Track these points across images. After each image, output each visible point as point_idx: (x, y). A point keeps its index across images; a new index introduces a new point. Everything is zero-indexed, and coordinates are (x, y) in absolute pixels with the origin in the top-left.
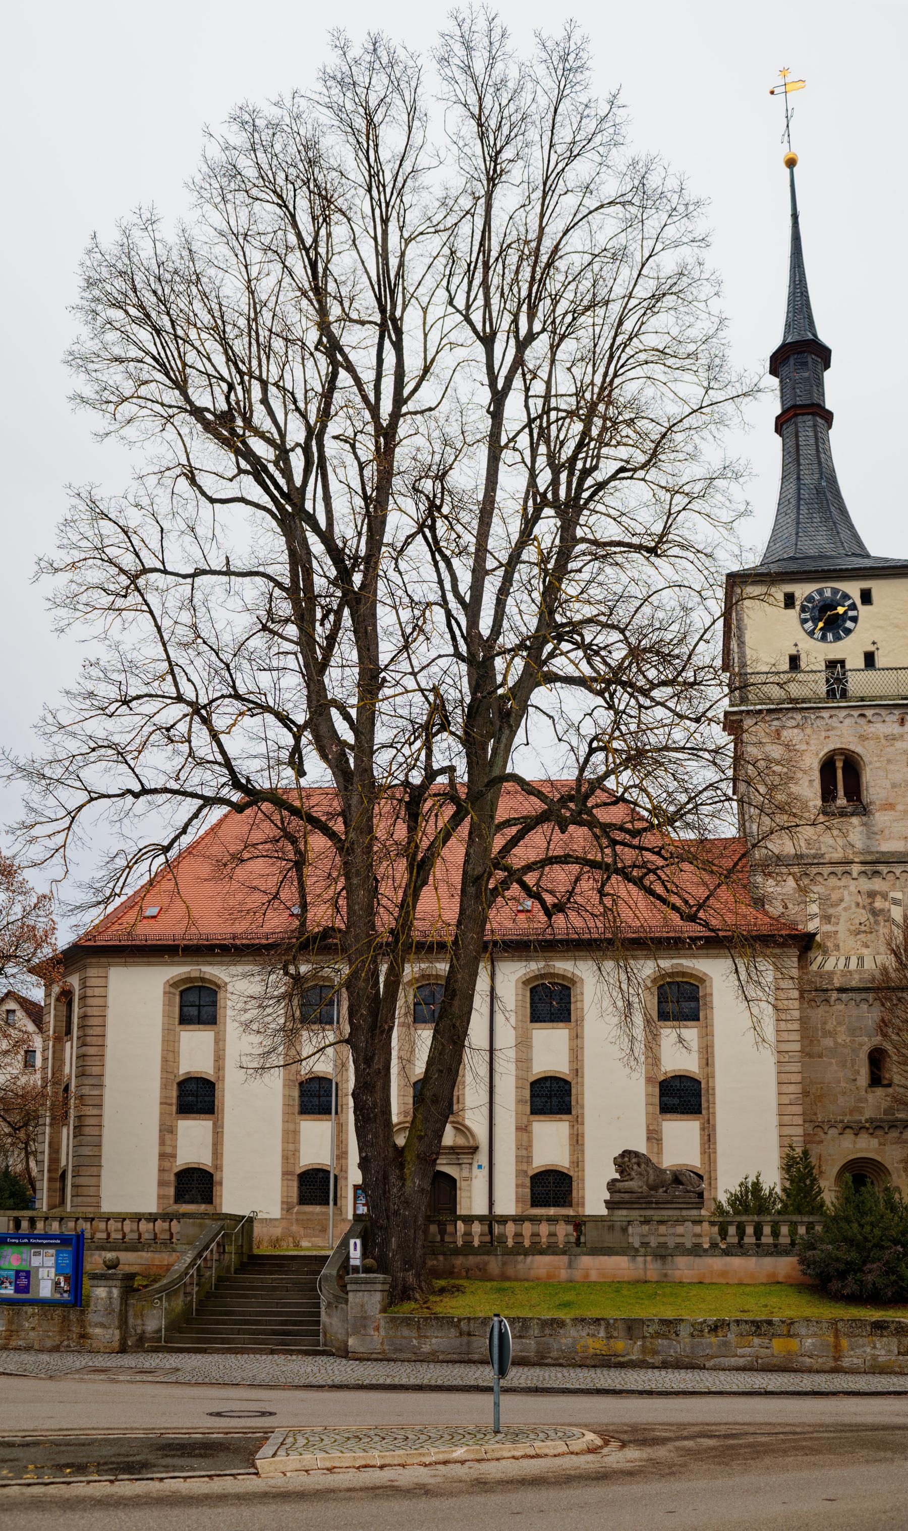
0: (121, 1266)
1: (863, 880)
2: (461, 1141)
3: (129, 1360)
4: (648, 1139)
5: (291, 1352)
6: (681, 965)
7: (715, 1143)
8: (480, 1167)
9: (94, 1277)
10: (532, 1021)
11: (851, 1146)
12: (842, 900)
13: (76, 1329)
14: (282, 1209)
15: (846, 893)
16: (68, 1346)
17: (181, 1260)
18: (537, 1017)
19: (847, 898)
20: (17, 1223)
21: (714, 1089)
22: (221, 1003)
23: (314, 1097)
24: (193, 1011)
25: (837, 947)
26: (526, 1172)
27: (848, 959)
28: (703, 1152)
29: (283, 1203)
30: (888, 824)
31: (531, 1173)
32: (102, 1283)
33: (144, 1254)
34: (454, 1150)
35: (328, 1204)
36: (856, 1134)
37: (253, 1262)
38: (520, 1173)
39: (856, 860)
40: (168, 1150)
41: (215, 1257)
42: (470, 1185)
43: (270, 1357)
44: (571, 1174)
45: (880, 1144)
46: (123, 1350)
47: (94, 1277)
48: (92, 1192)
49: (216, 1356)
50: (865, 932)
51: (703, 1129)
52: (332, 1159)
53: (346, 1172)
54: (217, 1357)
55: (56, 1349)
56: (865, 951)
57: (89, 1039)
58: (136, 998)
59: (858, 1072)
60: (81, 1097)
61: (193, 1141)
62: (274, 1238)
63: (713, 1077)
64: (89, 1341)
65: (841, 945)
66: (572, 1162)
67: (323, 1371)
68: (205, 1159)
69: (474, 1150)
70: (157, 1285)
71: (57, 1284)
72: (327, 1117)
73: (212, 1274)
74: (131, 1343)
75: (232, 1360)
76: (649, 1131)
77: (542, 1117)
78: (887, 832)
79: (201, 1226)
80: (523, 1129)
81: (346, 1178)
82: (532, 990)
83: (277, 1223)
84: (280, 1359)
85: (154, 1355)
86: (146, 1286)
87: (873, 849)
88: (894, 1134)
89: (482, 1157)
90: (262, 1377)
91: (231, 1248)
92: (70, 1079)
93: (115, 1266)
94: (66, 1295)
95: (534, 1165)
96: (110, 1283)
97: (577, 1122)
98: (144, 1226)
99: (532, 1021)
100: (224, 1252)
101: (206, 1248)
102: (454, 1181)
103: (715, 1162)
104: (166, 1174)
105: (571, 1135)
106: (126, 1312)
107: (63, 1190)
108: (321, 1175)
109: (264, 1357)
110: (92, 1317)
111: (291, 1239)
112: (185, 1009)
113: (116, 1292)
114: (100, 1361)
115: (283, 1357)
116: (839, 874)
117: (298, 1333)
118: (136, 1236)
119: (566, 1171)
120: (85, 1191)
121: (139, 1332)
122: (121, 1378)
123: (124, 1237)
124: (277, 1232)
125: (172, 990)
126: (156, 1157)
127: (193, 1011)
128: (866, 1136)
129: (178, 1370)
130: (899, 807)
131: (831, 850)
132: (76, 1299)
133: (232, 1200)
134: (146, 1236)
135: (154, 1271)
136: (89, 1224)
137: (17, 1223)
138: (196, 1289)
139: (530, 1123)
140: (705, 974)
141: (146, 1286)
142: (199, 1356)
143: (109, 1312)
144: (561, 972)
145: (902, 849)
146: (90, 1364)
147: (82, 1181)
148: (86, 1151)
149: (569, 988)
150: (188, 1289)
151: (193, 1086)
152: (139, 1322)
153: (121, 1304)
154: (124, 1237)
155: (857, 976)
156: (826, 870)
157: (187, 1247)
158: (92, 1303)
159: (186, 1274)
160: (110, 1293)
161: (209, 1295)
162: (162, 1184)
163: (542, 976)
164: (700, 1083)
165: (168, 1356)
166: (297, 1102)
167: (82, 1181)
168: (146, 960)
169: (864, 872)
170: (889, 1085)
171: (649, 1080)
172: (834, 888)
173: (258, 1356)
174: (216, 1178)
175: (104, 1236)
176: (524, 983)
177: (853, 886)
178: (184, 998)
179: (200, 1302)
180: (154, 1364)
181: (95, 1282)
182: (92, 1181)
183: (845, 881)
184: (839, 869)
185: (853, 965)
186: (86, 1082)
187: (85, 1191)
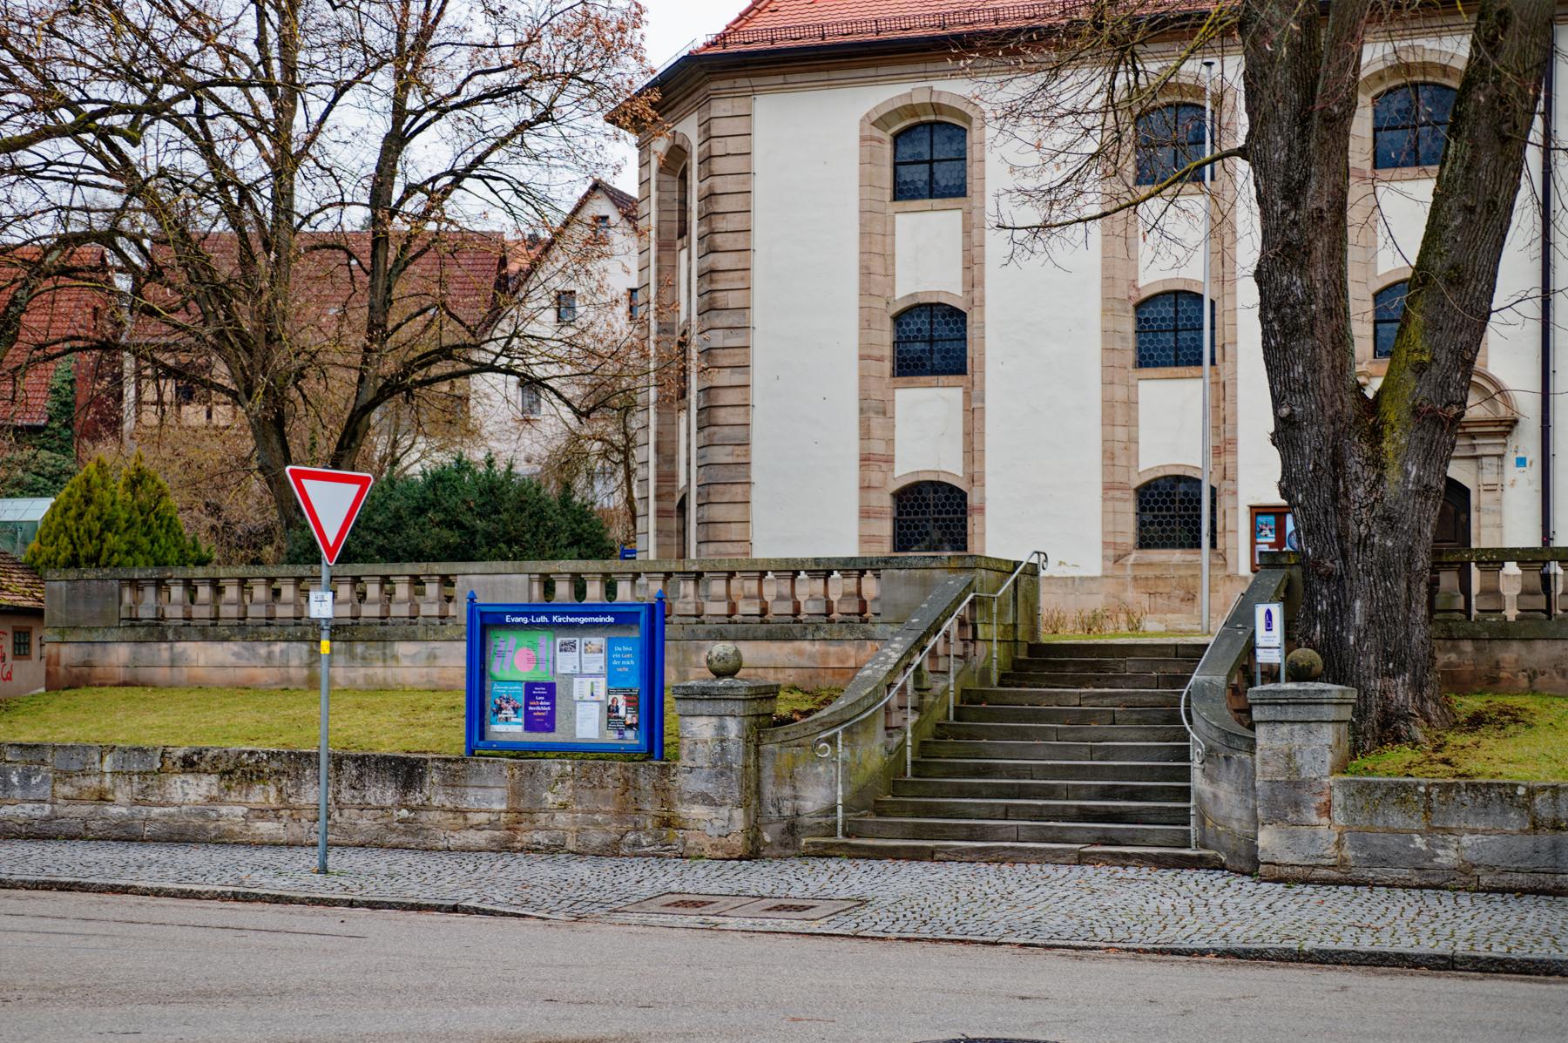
0: (741, 673)
3: (761, 878)
5: (1124, 860)
9: (687, 695)
13: (651, 807)
14: (1104, 557)
16: (637, 844)
17: (878, 658)
20: (548, 586)
22: (973, 153)
23: (1168, 331)
24: (919, 174)
29: (1105, 544)
32: (704, 707)
33: (806, 646)
35: (1199, 546)
37: (1039, 662)
40: (878, 447)
41: (956, 648)
43: (1077, 870)
46: (753, 853)
47: (687, 695)
48: (734, 532)
49: (954, 867)
54: (955, 872)
55: (611, 850)
57: (719, 239)
58: (808, 154)
60: (707, 353)
61: (927, 431)
62: (1088, 613)
64: (680, 833)
67: (1200, 910)
68: (947, 464)
70: (826, 711)
71: (612, 710)
72: (1193, 370)
73: (947, 688)
74: (772, 838)
75: (987, 878)
79: (926, 585)
83: (1094, 586)
84: (1097, 875)
85: (819, 864)
86: (808, 713)
90: (1055, 923)
91: (990, 631)
92: (689, 320)
93: (732, 673)
94: (630, 734)
96: (722, 707)
98: (807, 588)
100: (975, 638)
101: (934, 629)
104: (873, 495)
106: (759, 770)
107: (683, 532)
108: (1182, 487)
109: (1064, 870)
110: (691, 783)
111: (1123, 617)
112: (902, 169)
113: (733, 728)
114: (699, 879)
115: (1105, 871)
117: (1141, 816)
118: (787, 608)
120: (722, 532)
121: (787, 813)
122: (731, 923)
123: (764, 612)
124: (1095, 602)
126: (856, 462)
127: (919, 174)
129: (863, 903)
132: (654, 743)
133: (999, 535)
134: (808, 608)
135: (827, 681)
136: (691, 584)
137: (548, 586)
138: (912, 718)
141: (808, 713)
142: (917, 867)
143: (721, 769)
146: (675, 887)
147: (717, 512)
148: (720, 455)
150: (896, 720)
151: (921, 323)
152: (787, 791)
153: (747, 753)
154: (764, 612)
157: (896, 628)
158: (684, 752)
159: (890, 686)
160: (721, 728)
161: (942, 731)
162: (866, 514)
165: (847, 864)
166: (1131, 344)
167: (717, 512)
168: (824, 76)
173: (1049, 869)
174: (972, 500)
175: (723, 608)
178: (901, 149)
179: (922, 747)
180: (813, 888)
181: (690, 706)
182: (734, 513)
186: (717, 322)
187: (722, 532)
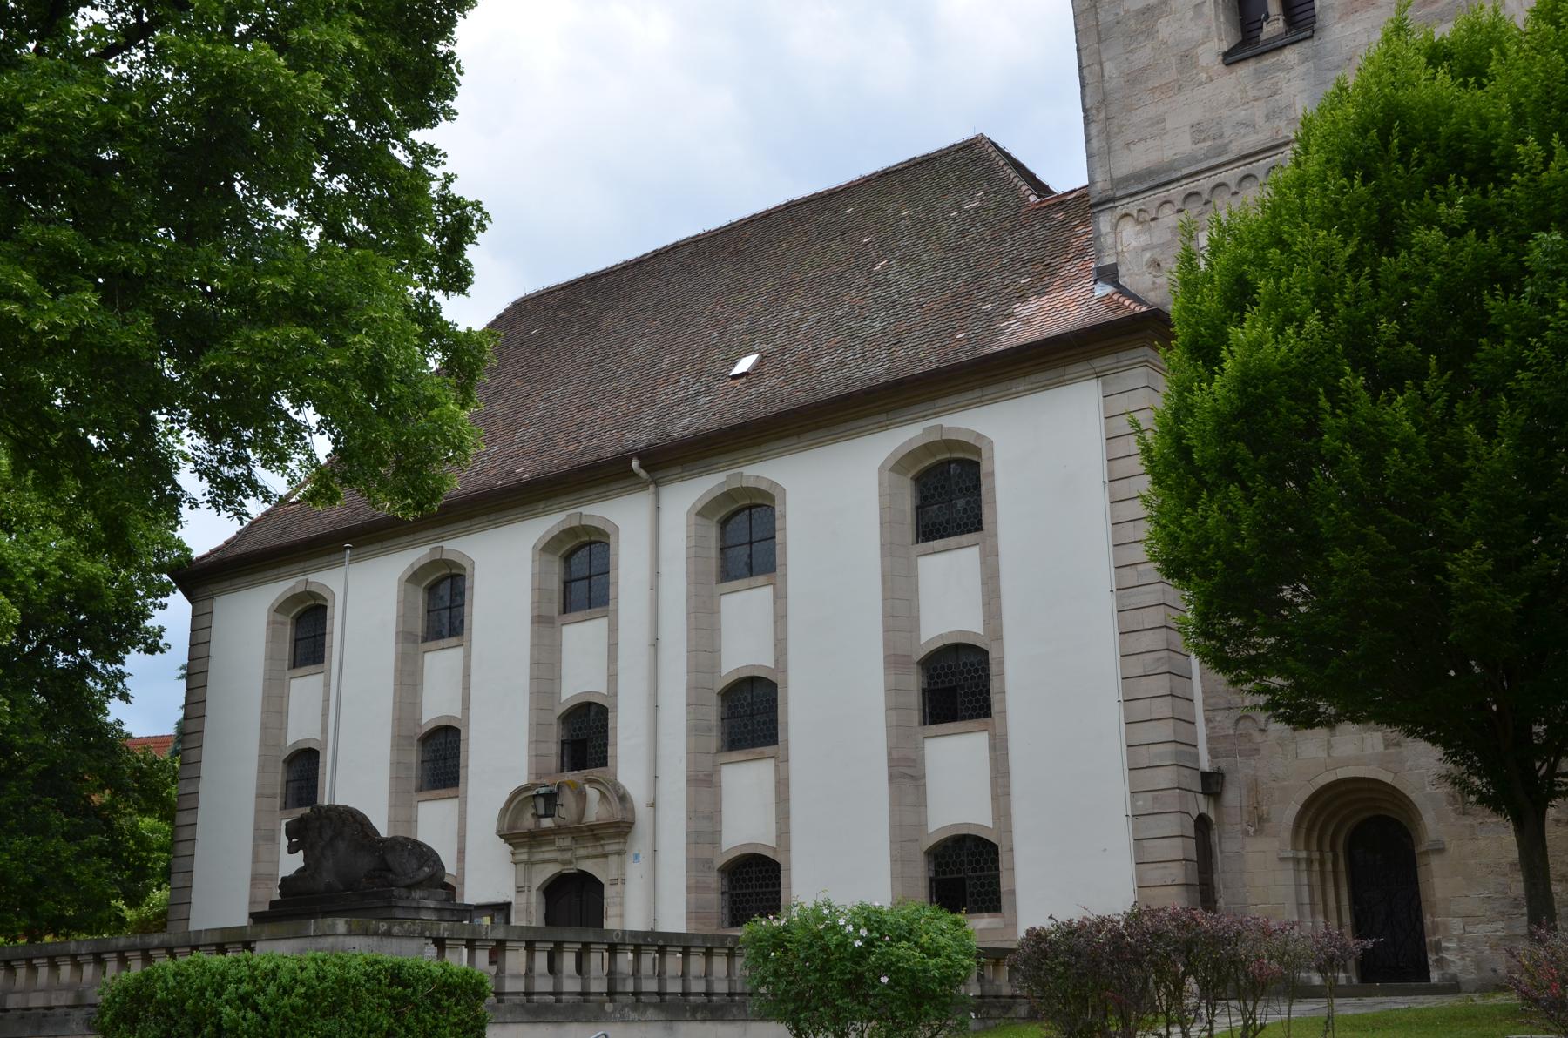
4: (891, 778)
11: (1322, 754)
26: (710, 861)
31: (720, 861)
76: (893, 762)
82: (724, 523)
95: (725, 848)
97: (782, 761)
119: (770, 854)
125: (280, 618)
131: (1243, 131)
144: (751, 484)
156: (1231, 175)
164: (984, 653)
171: (893, 661)
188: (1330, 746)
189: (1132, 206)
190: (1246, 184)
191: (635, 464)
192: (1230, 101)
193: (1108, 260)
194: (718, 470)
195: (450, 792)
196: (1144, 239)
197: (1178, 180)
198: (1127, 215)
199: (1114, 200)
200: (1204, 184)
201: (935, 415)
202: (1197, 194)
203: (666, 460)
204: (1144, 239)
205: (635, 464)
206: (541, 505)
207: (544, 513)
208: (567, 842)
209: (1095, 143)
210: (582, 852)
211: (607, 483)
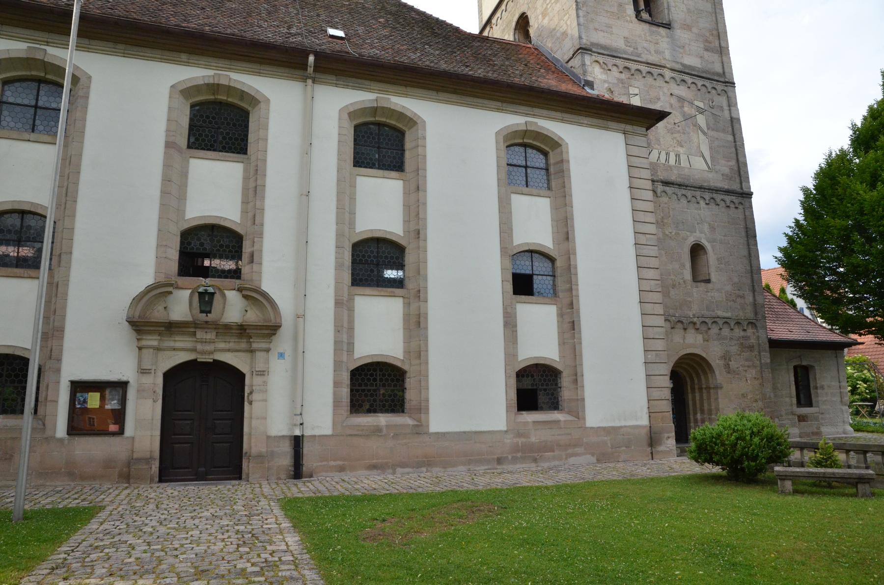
1: (673, 85)
2: (253, 316)
6: (536, 123)
7: (580, 332)
8: (281, 355)
10: (354, 166)
11: (682, 341)
12: (659, 99)
15: (661, 93)
18: (361, 161)
19: (662, 98)
21: (576, 268)
25: (658, 140)
27: (668, 154)
28: (562, 343)
30: (687, 41)
34: (242, 331)
36: (685, 329)
38: (338, 365)
39: (668, 66)
42: (265, 383)
44: (405, 367)
45: (705, 340)
50: (679, 132)
51: (561, 315)
52: (34, 343)
53: (59, 360)
56: (681, 150)
59: (683, 266)
63: (575, 254)
65: (661, 140)
66: (407, 352)
69: (271, 330)
77: (368, 290)
78: (687, 48)
80: (344, 307)
81: (58, 371)
82: (357, 128)
87: (678, 60)
88: (714, 330)
89: (283, 342)
99: (354, 166)
102: (243, 376)
103: (581, 355)
105: (407, 318)
116: (655, 75)
119: (399, 364)
128: (693, 331)
130: (694, 30)
139: (351, 299)
140: (560, 138)
145: (699, 66)
149: (402, 133)
155: (675, 172)
163: (375, 110)
169: (673, 78)
170: (708, 281)
172: (651, 86)
176: (350, 114)
177: (666, 89)
183: (660, 82)
184: (655, 71)
185: (672, 161)
188: (684, 338)
189: (601, 59)
190: (649, 76)
191: (311, 58)
192: (640, 36)
193: (590, 79)
194: (370, 90)
195: (31, 272)
196: (604, 77)
197: (620, 58)
198: (597, 61)
199: (591, 50)
200: (633, 66)
201: (534, 116)
202: (628, 68)
203: (338, 66)
204: (604, 77)
205: (311, 58)
206: (184, 57)
207: (187, 64)
208: (211, 336)
209: (582, 20)
210: (222, 345)
211: (261, 63)
